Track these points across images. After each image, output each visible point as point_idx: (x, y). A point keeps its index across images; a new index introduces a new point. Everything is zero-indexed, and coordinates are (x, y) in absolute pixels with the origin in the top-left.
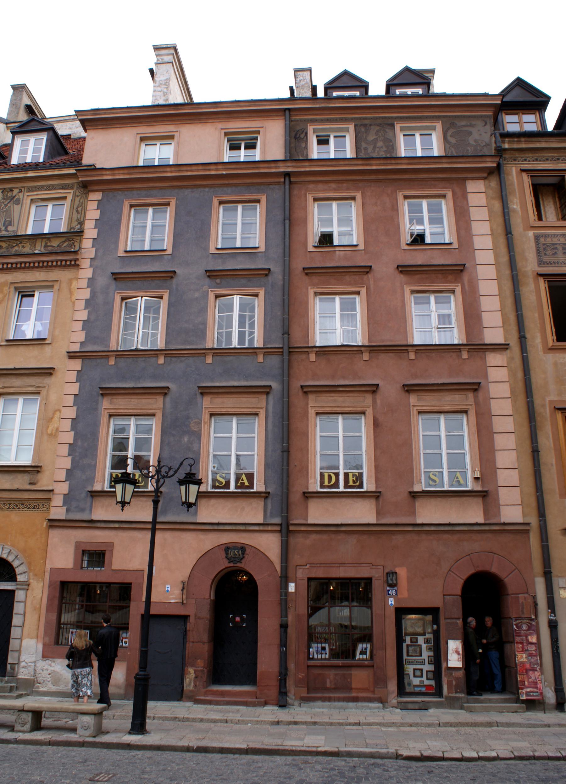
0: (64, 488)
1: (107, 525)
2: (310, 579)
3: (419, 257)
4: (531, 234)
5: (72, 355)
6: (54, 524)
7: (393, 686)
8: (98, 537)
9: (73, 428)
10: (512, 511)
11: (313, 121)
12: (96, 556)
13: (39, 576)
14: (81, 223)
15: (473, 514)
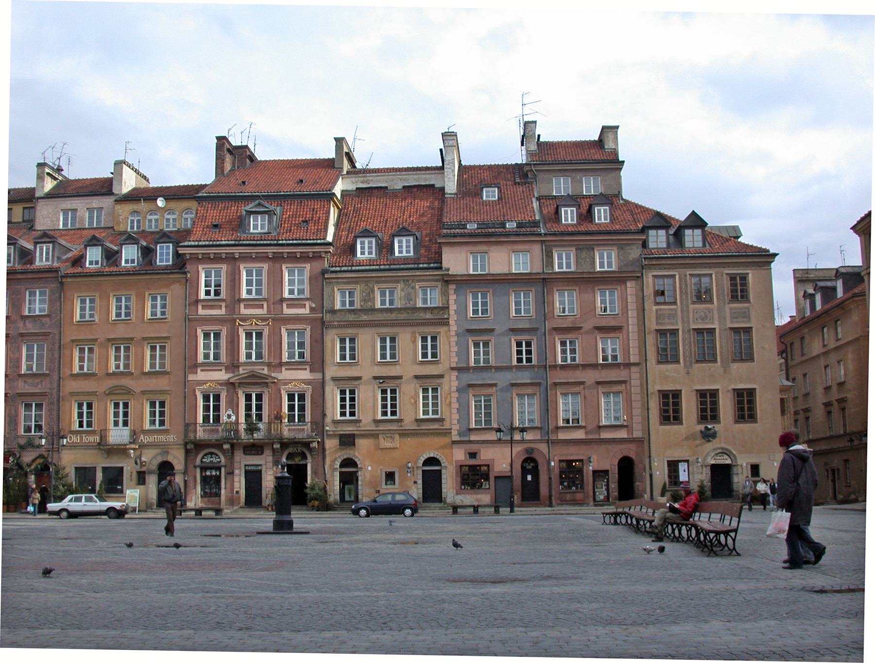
0: (457, 427)
1: (477, 442)
2: (560, 461)
3: (603, 323)
4: (654, 308)
5: (453, 369)
6: (454, 442)
7: (591, 499)
8: (473, 448)
9: (458, 401)
10: (637, 434)
11: (556, 246)
12: (473, 455)
13: (451, 463)
14: (448, 302)
15: (623, 434)
